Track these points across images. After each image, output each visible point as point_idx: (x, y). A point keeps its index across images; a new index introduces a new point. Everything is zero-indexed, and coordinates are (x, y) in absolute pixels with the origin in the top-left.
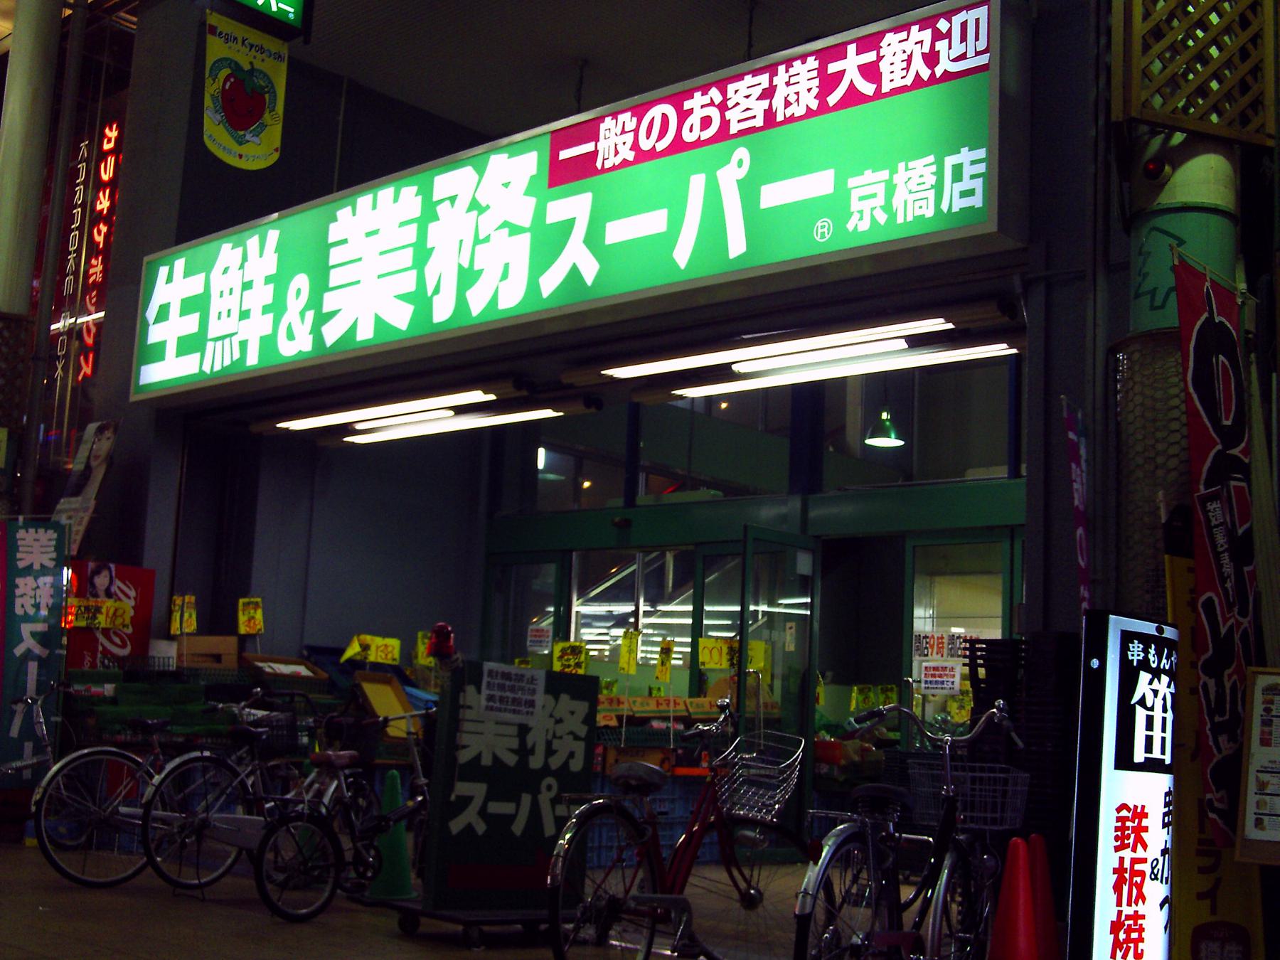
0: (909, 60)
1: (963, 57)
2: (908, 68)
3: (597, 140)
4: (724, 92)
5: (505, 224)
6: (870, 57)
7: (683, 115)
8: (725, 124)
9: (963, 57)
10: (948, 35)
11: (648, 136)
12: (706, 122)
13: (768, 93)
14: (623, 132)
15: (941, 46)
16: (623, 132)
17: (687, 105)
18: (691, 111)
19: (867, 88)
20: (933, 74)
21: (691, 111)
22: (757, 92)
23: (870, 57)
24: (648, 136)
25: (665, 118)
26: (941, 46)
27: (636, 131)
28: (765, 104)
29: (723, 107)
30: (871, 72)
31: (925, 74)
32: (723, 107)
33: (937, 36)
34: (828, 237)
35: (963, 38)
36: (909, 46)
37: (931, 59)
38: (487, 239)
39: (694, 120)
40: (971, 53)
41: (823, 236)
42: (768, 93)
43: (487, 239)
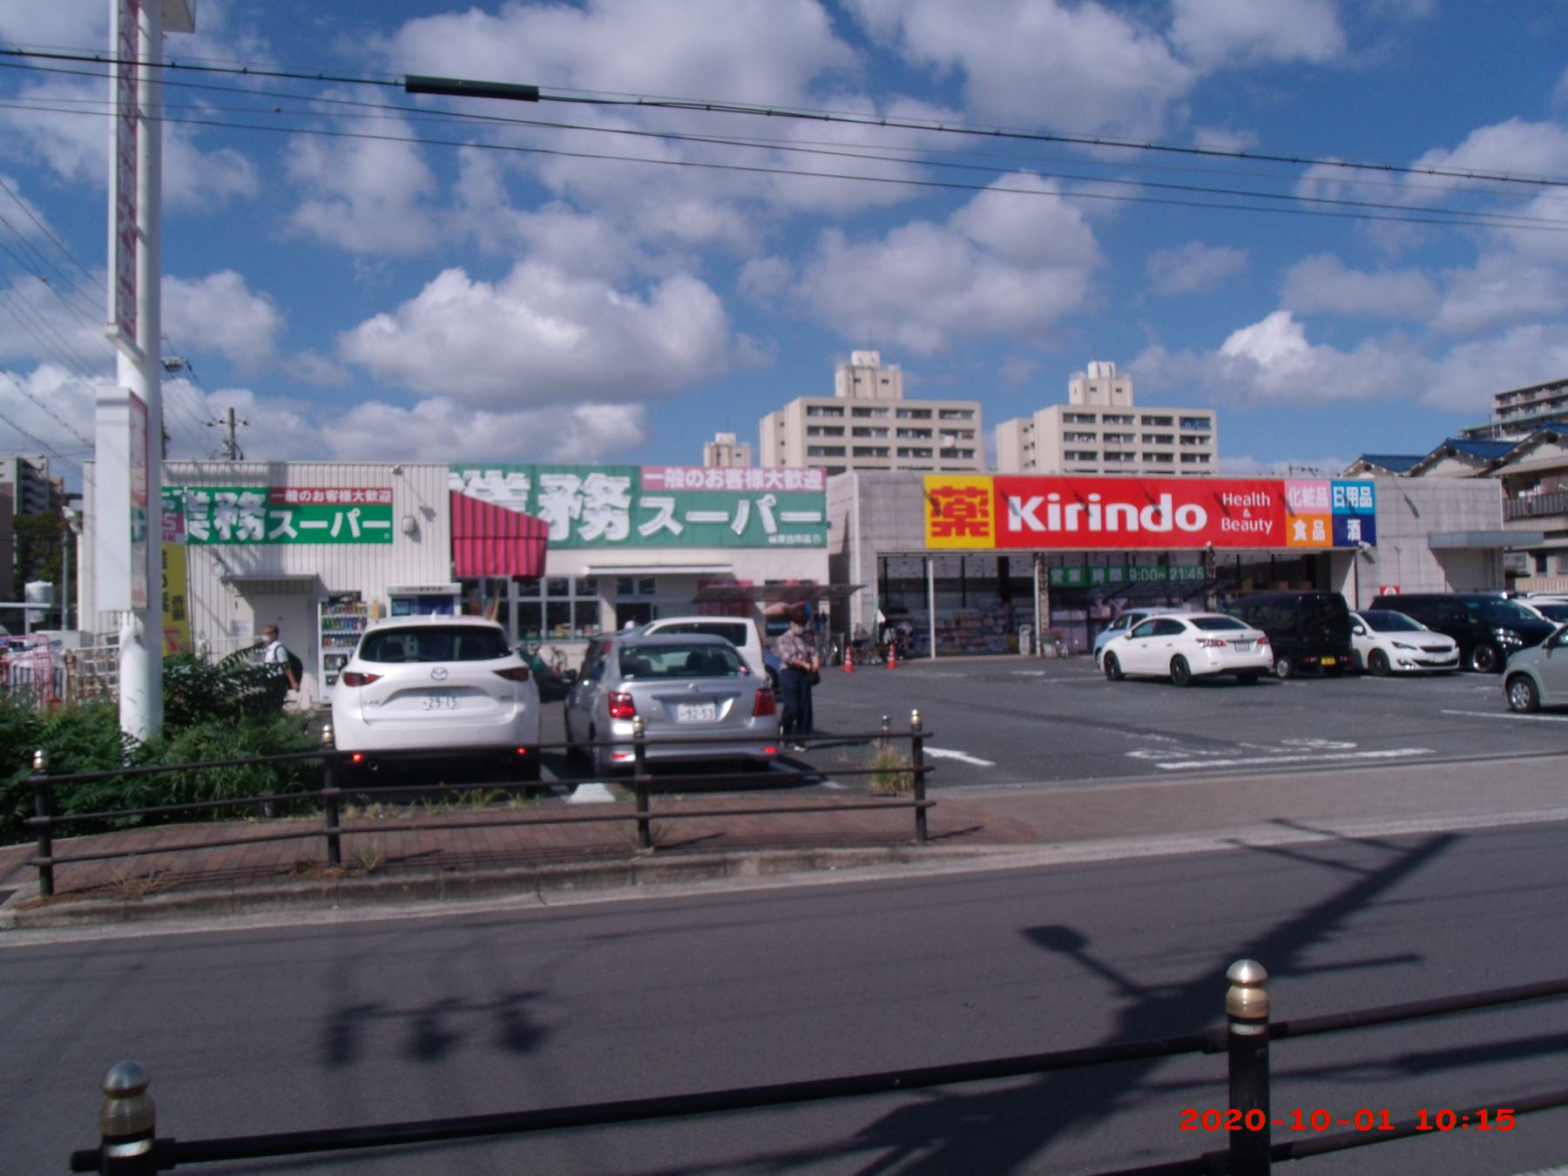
7: (706, 477)
8: (725, 485)
12: (717, 482)
13: (744, 477)
23: (780, 475)
29: (724, 477)
33: (804, 476)
37: (803, 482)
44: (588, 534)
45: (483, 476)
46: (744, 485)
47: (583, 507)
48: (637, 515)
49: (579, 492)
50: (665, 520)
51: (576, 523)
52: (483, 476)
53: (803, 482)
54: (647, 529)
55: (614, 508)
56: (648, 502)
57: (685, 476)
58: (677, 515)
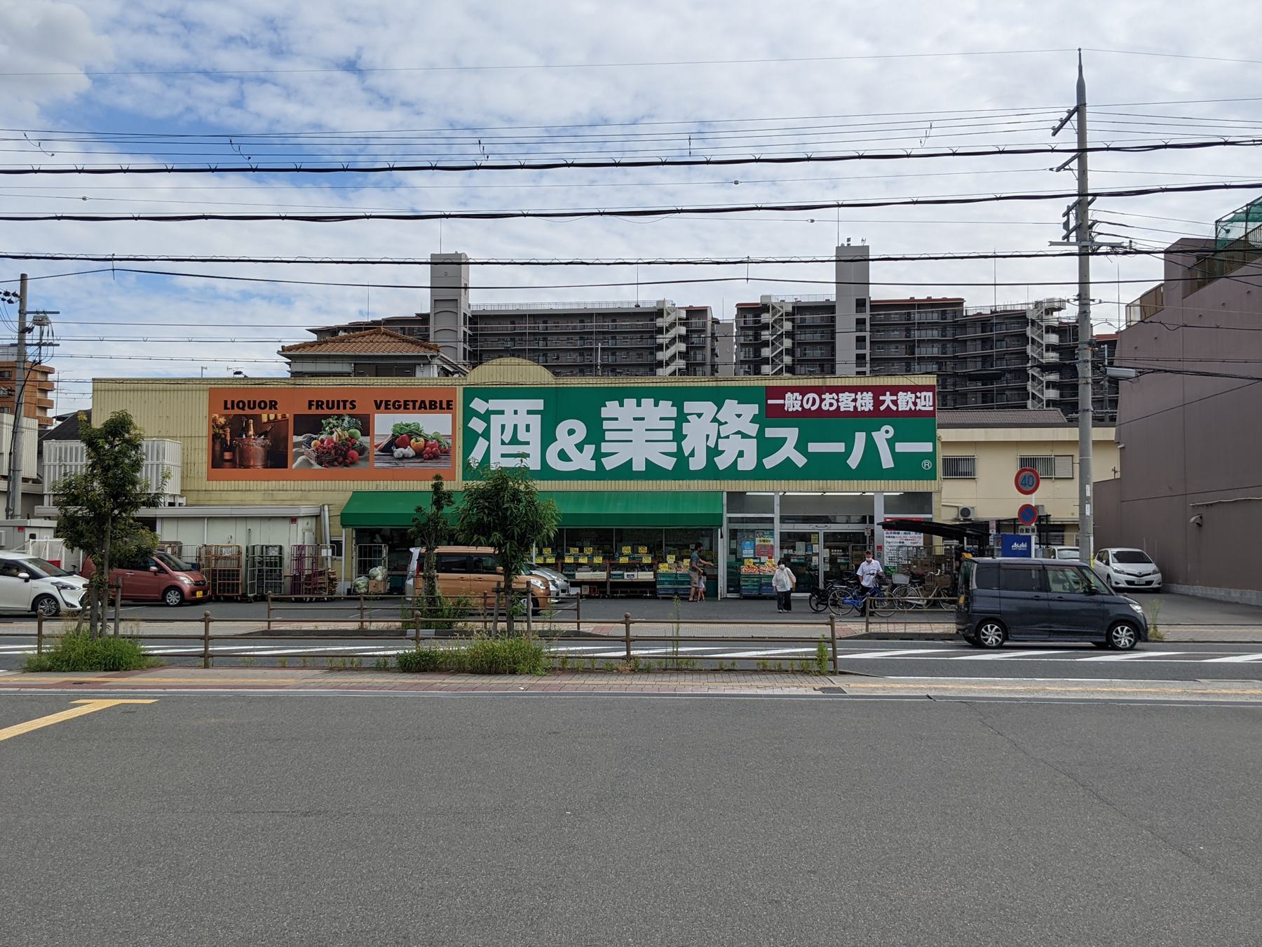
0: (908, 402)
1: (925, 406)
2: (907, 405)
3: (785, 400)
4: (838, 396)
5: (738, 432)
6: (894, 398)
7: (822, 400)
8: (838, 407)
9: (925, 406)
10: (920, 398)
11: (807, 403)
12: (831, 405)
13: (855, 400)
14: (796, 399)
15: (918, 400)
16: (796, 399)
17: (823, 396)
18: (825, 399)
19: (894, 408)
20: (915, 409)
21: (825, 399)
22: (851, 399)
23: (894, 398)
24: (807, 403)
25: (814, 399)
26: (918, 400)
27: (802, 400)
28: (854, 404)
29: (838, 401)
30: (895, 403)
31: (913, 408)
32: (838, 401)
33: (917, 397)
34: (929, 468)
35: (925, 400)
36: (907, 398)
37: (915, 404)
38: (727, 437)
39: (827, 402)
40: (927, 405)
41: (927, 467)
42: (855, 400)
43: (727, 437)
44: (722, 463)
45: (639, 405)
46: (855, 407)
47: (719, 437)
48: (767, 447)
49: (715, 420)
50: (788, 451)
51: (713, 452)
52: (639, 405)
53: (915, 404)
54: (770, 462)
55: (745, 436)
56: (771, 433)
57: (802, 400)
58: (801, 447)
